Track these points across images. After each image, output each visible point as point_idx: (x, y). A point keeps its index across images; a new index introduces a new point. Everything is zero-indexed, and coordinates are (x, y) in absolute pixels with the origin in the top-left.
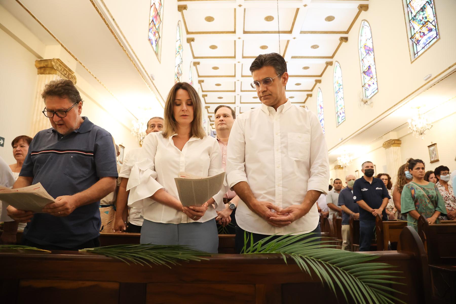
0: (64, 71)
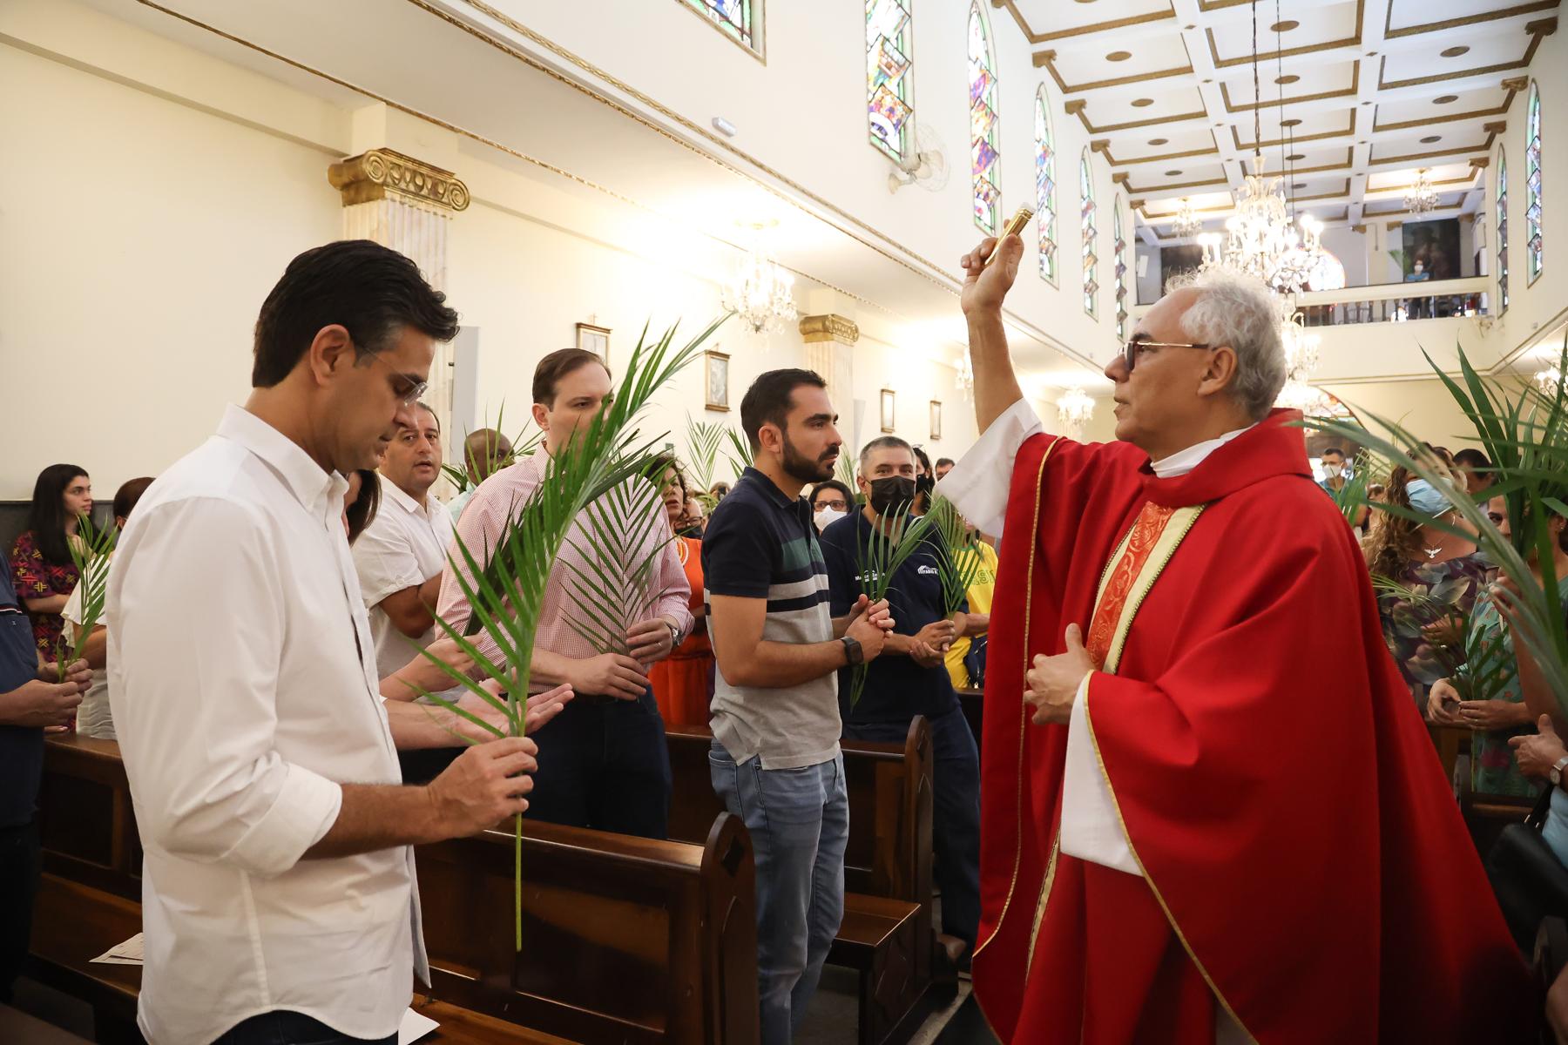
0: (413, 180)
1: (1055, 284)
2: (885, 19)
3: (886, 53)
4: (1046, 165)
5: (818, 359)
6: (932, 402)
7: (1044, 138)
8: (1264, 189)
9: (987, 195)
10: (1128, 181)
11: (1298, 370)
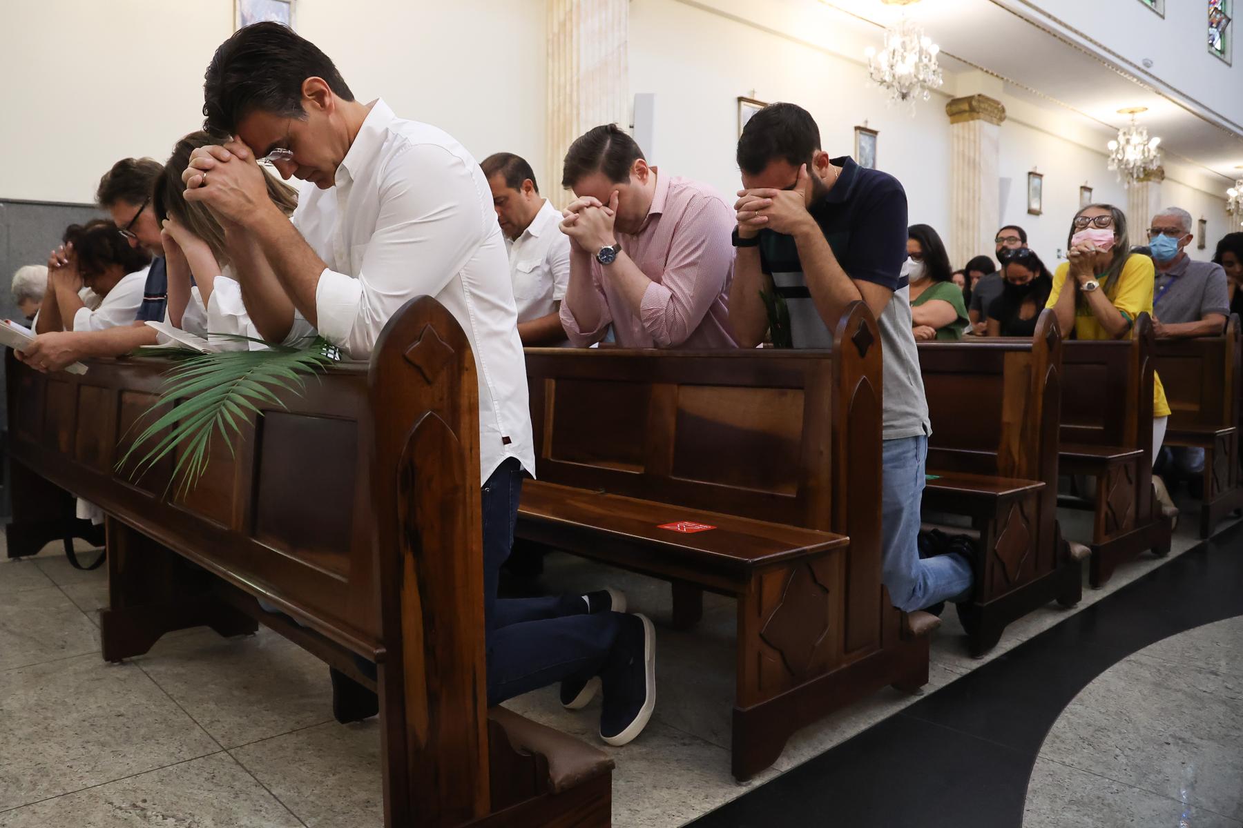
1: (1227, 58)
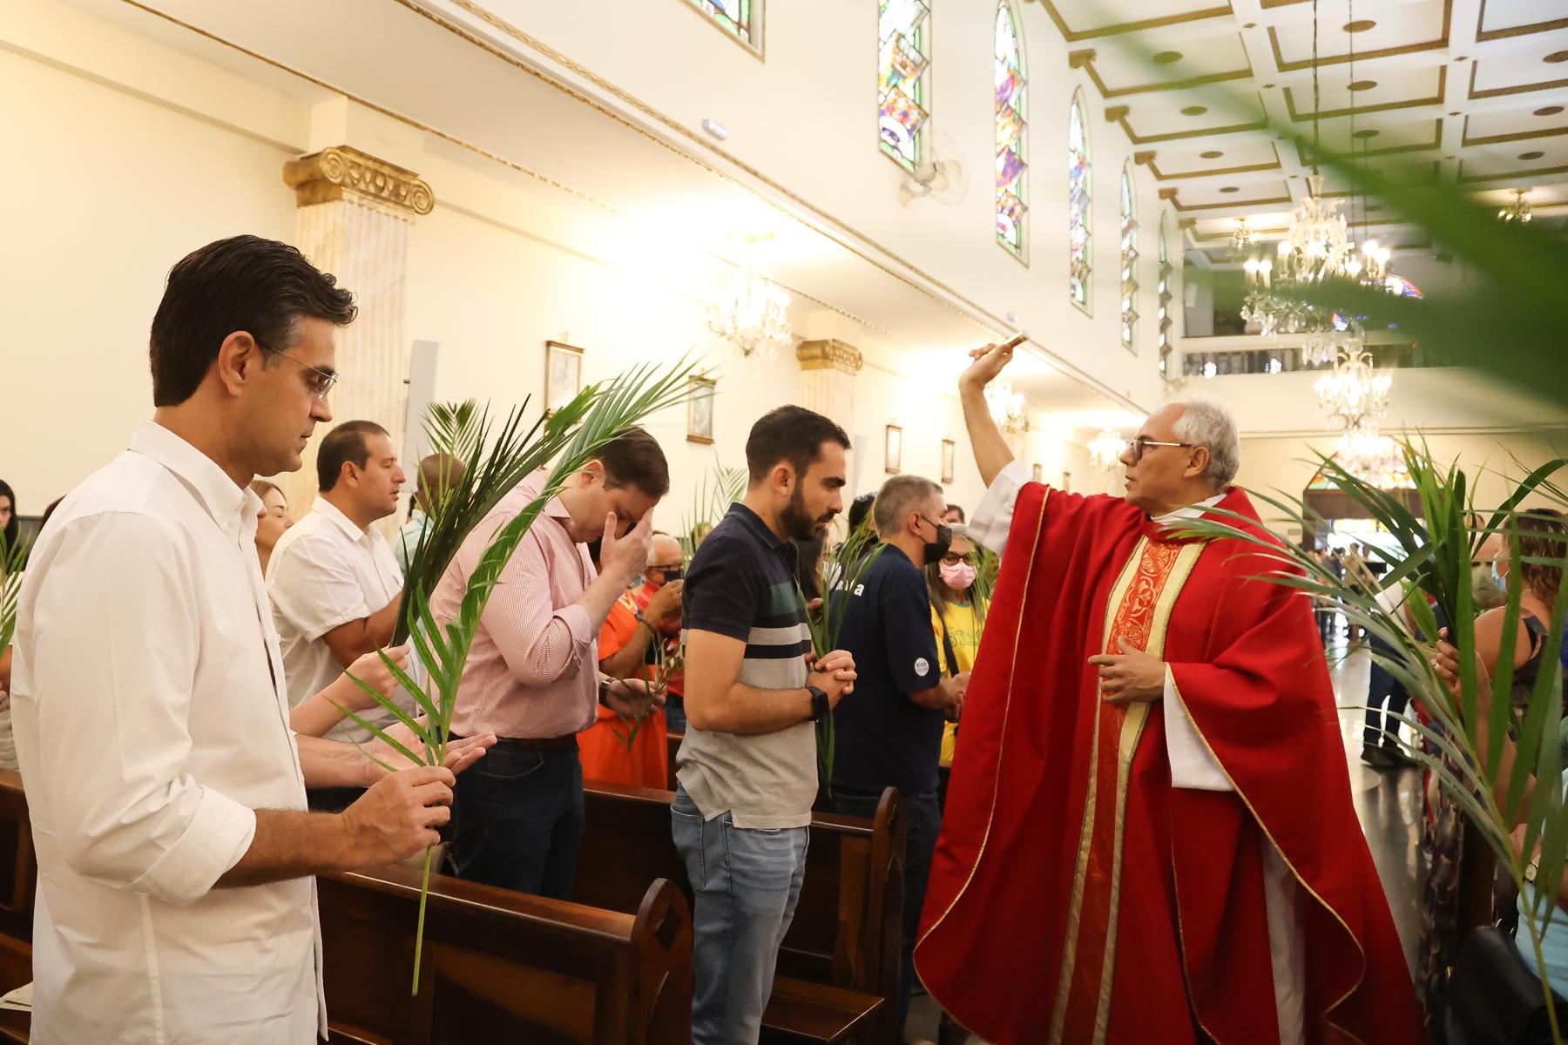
0: (373, 180)
1: (1089, 312)
2: (901, 14)
3: (900, 50)
4: (1081, 179)
5: (815, 389)
6: (944, 441)
7: (1080, 148)
8: (1322, 211)
9: (1012, 211)
10: (1177, 197)
11: (1364, 417)
